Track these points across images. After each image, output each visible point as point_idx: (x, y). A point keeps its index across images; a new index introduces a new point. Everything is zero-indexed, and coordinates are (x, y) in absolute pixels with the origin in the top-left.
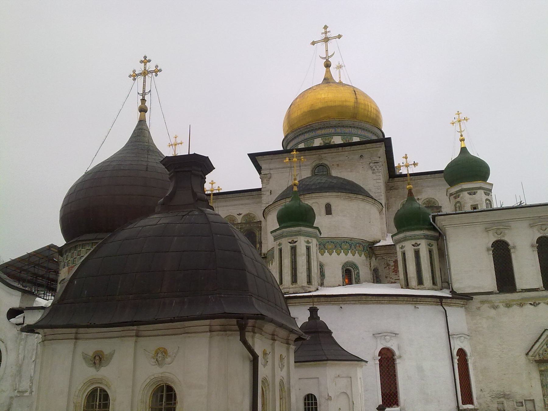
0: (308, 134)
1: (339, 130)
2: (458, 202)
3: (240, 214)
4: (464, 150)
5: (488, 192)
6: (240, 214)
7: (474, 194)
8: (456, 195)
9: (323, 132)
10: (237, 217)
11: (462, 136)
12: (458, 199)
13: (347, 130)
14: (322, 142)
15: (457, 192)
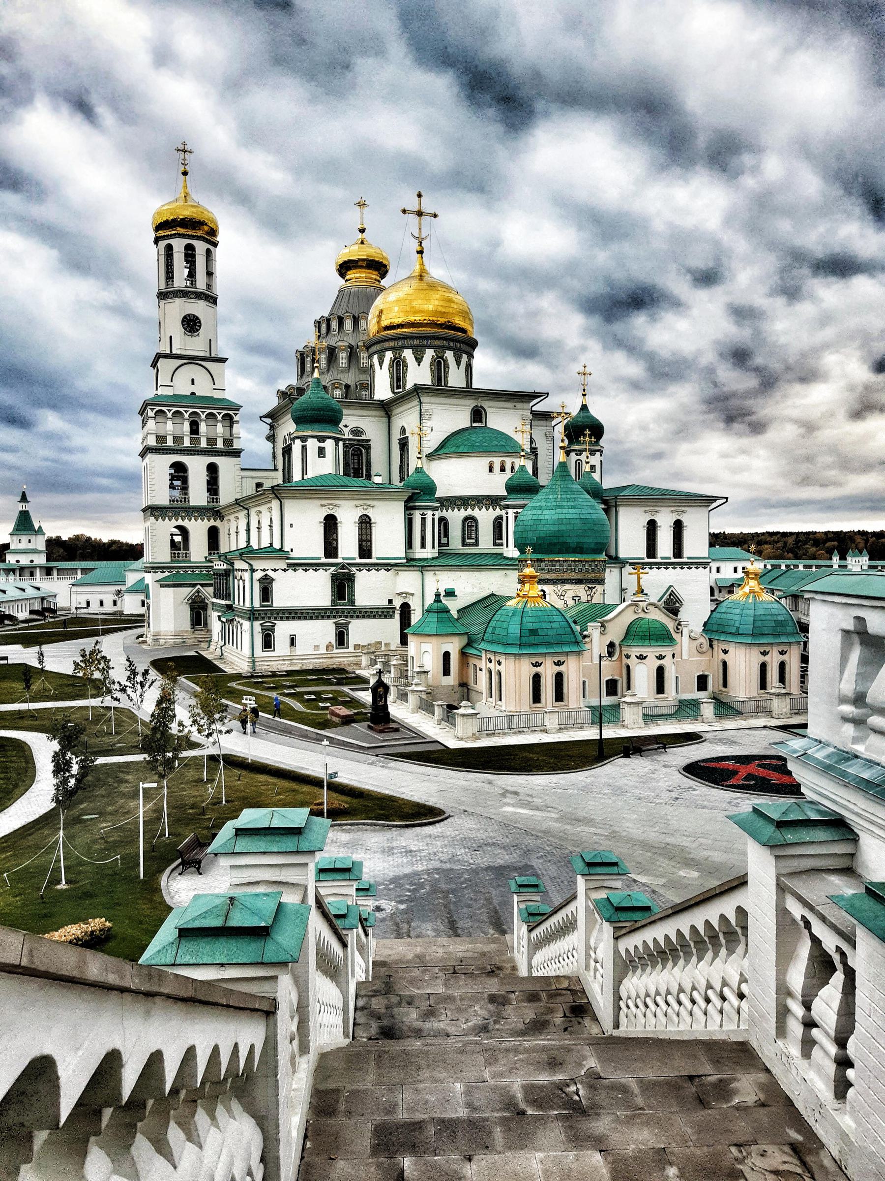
0: (418, 341)
1: (452, 344)
2: (579, 460)
3: (346, 426)
4: (584, 408)
5: (601, 452)
6: (346, 426)
7: (594, 454)
8: (579, 453)
9: (437, 343)
10: (343, 428)
11: (584, 390)
12: (579, 457)
13: (459, 345)
14: (434, 354)
15: (580, 450)
